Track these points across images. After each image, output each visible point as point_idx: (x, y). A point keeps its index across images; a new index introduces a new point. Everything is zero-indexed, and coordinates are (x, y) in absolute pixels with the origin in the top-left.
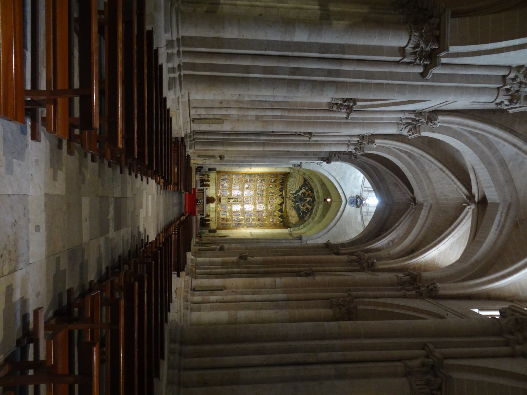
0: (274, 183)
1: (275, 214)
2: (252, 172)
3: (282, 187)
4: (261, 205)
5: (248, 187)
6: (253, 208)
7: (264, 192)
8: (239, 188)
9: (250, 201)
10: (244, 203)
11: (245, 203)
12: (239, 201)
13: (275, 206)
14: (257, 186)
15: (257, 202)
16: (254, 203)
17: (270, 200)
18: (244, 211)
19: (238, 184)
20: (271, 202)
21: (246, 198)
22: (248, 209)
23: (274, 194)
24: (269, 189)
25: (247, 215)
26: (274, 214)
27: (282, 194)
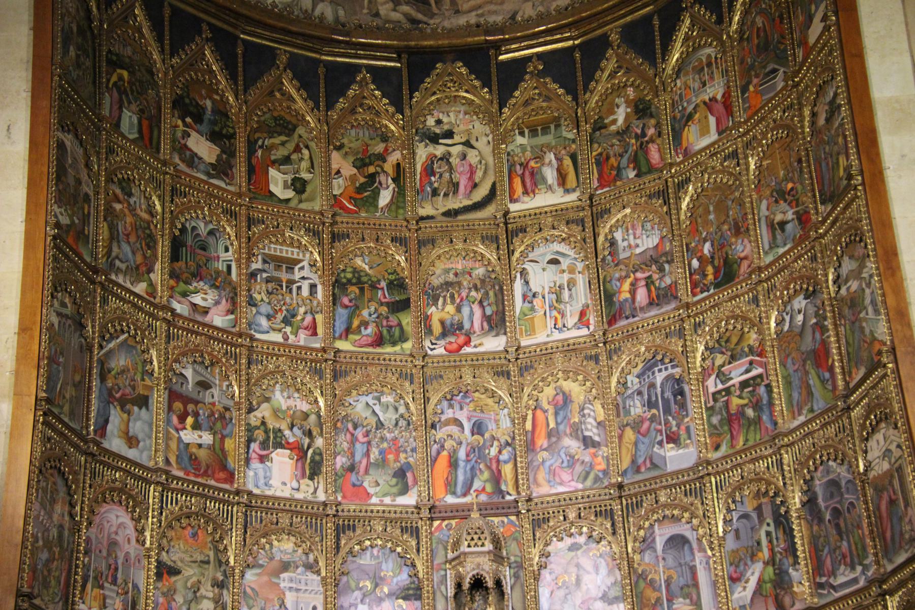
0: (241, 145)
1: (621, 115)
2: (23, 329)
3: (284, 58)
4: (529, 297)
5: (300, 452)
6: (573, 388)
7: (359, 262)
8: (311, 567)
9: (478, 428)
10: (512, 509)
11: (507, 485)
12: (486, 568)
13: (520, 140)
14: (277, 337)
15: (494, 344)
16: (508, 375)
17: (454, 203)
18: (620, 486)
19: (250, 575)
20: (475, 186)
21: (450, 487)
22: (587, 442)
23: (382, 157)
24: (317, 206)
25: (673, 439)
26: (622, 133)
27: (370, 69)
